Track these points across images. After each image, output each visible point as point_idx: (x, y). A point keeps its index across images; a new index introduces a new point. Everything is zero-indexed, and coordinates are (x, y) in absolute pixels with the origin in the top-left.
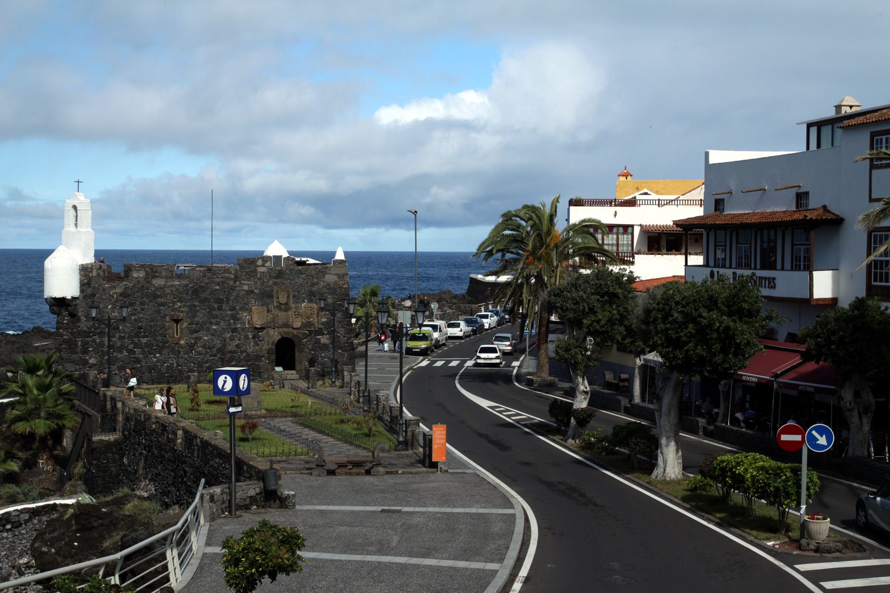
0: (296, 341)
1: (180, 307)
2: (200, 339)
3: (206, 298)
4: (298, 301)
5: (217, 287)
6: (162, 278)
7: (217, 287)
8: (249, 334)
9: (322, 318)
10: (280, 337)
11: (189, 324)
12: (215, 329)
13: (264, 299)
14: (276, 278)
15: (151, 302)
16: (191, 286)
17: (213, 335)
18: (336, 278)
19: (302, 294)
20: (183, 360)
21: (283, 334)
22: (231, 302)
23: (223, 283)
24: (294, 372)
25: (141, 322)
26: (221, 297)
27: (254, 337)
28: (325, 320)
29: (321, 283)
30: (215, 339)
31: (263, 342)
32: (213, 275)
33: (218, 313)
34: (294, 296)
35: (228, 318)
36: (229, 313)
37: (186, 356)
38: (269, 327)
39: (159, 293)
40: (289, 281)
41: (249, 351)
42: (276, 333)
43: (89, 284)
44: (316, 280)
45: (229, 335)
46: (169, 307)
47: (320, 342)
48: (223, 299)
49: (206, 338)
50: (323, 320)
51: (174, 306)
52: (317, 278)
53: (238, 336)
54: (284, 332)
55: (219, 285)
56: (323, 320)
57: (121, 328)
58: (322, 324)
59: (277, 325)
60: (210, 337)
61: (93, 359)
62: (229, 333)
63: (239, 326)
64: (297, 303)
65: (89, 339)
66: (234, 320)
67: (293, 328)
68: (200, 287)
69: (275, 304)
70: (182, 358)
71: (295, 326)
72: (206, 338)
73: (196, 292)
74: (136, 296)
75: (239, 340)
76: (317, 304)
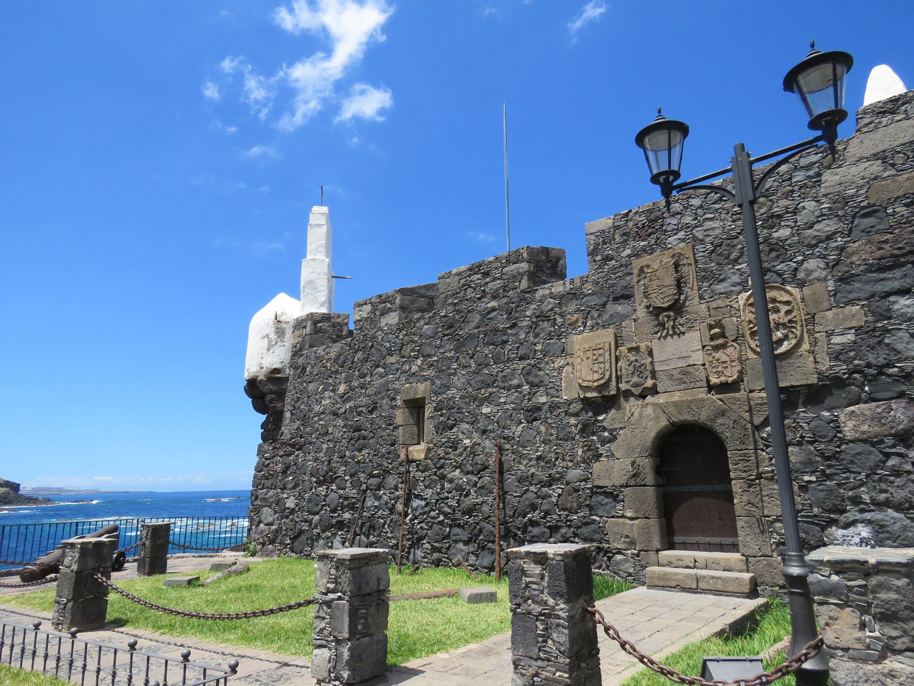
0: (722, 427)
1: (421, 369)
2: (454, 445)
3: (471, 337)
4: (720, 287)
5: (494, 304)
6: (395, 311)
7: (494, 304)
8: (573, 421)
9: (830, 334)
10: (664, 423)
11: (436, 410)
12: (487, 416)
13: (609, 306)
14: (639, 236)
15: (378, 366)
16: (443, 314)
17: (484, 432)
18: (876, 167)
19: (736, 261)
20: (423, 503)
21: (671, 410)
22: (522, 336)
23: (504, 288)
24: (734, 557)
25: (359, 414)
26: (501, 326)
27: (586, 429)
28: (850, 337)
29: (810, 205)
30: (487, 442)
31: (613, 446)
32: (486, 274)
33: (495, 369)
34: (706, 277)
35: (515, 382)
36: (521, 365)
37: (429, 492)
38: (627, 394)
39: (388, 345)
40: (681, 234)
41: (574, 474)
42: (649, 410)
43: (301, 349)
44: (784, 203)
45: (520, 428)
46: (401, 373)
47: (838, 429)
48: (504, 331)
49: (467, 441)
50: (836, 340)
51: (410, 368)
52: (788, 195)
53: (543, 429)
54: (676, 404)
55: (494, 297)
56: (836, 340)
57: (330, 430)
58: (836, 356)
59: (649, 383)
60: (476, 437)
61: (292, 498)
62: (522, 423)
63: (543, 399)
64: (714, 295)
65: (291, 458)
66: (532, 385)
67: (711, 388)
68: (458, 312)
69: (641, 313)
70: (421, 498)
71: (714, 380)
72: (467, 441)
73: (450, 327)
74: (356, 359)
75: (544, 442)
76: (801, 285)
